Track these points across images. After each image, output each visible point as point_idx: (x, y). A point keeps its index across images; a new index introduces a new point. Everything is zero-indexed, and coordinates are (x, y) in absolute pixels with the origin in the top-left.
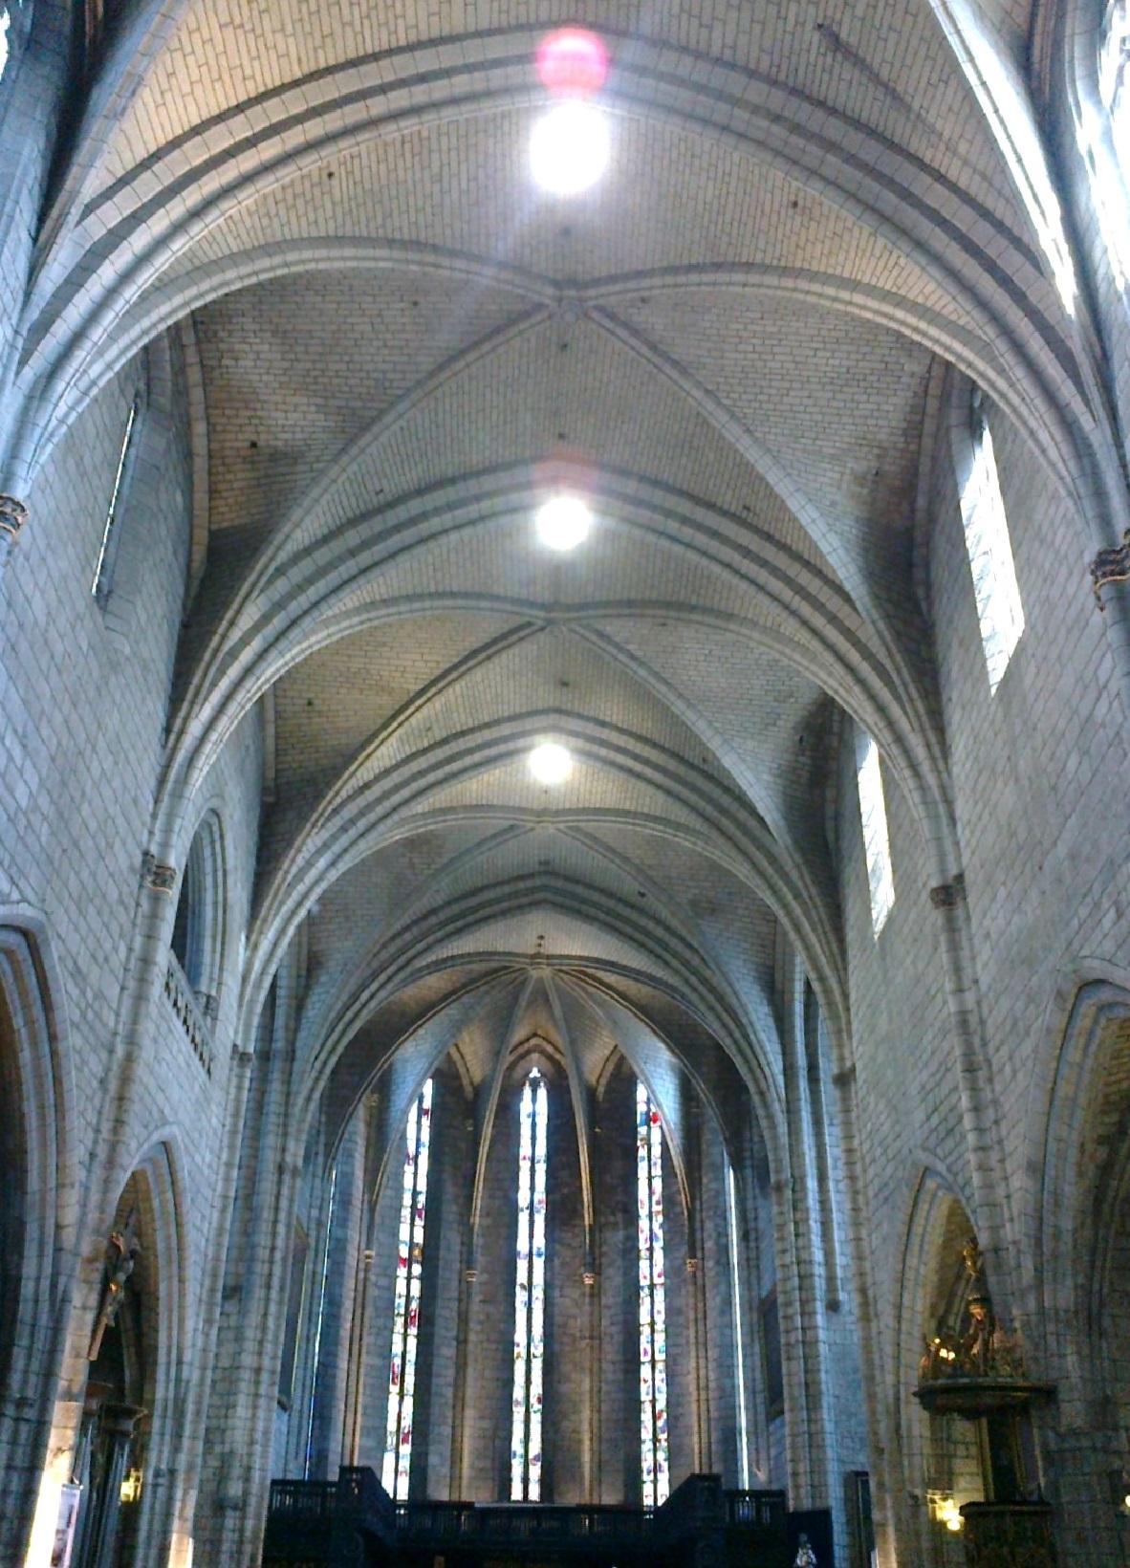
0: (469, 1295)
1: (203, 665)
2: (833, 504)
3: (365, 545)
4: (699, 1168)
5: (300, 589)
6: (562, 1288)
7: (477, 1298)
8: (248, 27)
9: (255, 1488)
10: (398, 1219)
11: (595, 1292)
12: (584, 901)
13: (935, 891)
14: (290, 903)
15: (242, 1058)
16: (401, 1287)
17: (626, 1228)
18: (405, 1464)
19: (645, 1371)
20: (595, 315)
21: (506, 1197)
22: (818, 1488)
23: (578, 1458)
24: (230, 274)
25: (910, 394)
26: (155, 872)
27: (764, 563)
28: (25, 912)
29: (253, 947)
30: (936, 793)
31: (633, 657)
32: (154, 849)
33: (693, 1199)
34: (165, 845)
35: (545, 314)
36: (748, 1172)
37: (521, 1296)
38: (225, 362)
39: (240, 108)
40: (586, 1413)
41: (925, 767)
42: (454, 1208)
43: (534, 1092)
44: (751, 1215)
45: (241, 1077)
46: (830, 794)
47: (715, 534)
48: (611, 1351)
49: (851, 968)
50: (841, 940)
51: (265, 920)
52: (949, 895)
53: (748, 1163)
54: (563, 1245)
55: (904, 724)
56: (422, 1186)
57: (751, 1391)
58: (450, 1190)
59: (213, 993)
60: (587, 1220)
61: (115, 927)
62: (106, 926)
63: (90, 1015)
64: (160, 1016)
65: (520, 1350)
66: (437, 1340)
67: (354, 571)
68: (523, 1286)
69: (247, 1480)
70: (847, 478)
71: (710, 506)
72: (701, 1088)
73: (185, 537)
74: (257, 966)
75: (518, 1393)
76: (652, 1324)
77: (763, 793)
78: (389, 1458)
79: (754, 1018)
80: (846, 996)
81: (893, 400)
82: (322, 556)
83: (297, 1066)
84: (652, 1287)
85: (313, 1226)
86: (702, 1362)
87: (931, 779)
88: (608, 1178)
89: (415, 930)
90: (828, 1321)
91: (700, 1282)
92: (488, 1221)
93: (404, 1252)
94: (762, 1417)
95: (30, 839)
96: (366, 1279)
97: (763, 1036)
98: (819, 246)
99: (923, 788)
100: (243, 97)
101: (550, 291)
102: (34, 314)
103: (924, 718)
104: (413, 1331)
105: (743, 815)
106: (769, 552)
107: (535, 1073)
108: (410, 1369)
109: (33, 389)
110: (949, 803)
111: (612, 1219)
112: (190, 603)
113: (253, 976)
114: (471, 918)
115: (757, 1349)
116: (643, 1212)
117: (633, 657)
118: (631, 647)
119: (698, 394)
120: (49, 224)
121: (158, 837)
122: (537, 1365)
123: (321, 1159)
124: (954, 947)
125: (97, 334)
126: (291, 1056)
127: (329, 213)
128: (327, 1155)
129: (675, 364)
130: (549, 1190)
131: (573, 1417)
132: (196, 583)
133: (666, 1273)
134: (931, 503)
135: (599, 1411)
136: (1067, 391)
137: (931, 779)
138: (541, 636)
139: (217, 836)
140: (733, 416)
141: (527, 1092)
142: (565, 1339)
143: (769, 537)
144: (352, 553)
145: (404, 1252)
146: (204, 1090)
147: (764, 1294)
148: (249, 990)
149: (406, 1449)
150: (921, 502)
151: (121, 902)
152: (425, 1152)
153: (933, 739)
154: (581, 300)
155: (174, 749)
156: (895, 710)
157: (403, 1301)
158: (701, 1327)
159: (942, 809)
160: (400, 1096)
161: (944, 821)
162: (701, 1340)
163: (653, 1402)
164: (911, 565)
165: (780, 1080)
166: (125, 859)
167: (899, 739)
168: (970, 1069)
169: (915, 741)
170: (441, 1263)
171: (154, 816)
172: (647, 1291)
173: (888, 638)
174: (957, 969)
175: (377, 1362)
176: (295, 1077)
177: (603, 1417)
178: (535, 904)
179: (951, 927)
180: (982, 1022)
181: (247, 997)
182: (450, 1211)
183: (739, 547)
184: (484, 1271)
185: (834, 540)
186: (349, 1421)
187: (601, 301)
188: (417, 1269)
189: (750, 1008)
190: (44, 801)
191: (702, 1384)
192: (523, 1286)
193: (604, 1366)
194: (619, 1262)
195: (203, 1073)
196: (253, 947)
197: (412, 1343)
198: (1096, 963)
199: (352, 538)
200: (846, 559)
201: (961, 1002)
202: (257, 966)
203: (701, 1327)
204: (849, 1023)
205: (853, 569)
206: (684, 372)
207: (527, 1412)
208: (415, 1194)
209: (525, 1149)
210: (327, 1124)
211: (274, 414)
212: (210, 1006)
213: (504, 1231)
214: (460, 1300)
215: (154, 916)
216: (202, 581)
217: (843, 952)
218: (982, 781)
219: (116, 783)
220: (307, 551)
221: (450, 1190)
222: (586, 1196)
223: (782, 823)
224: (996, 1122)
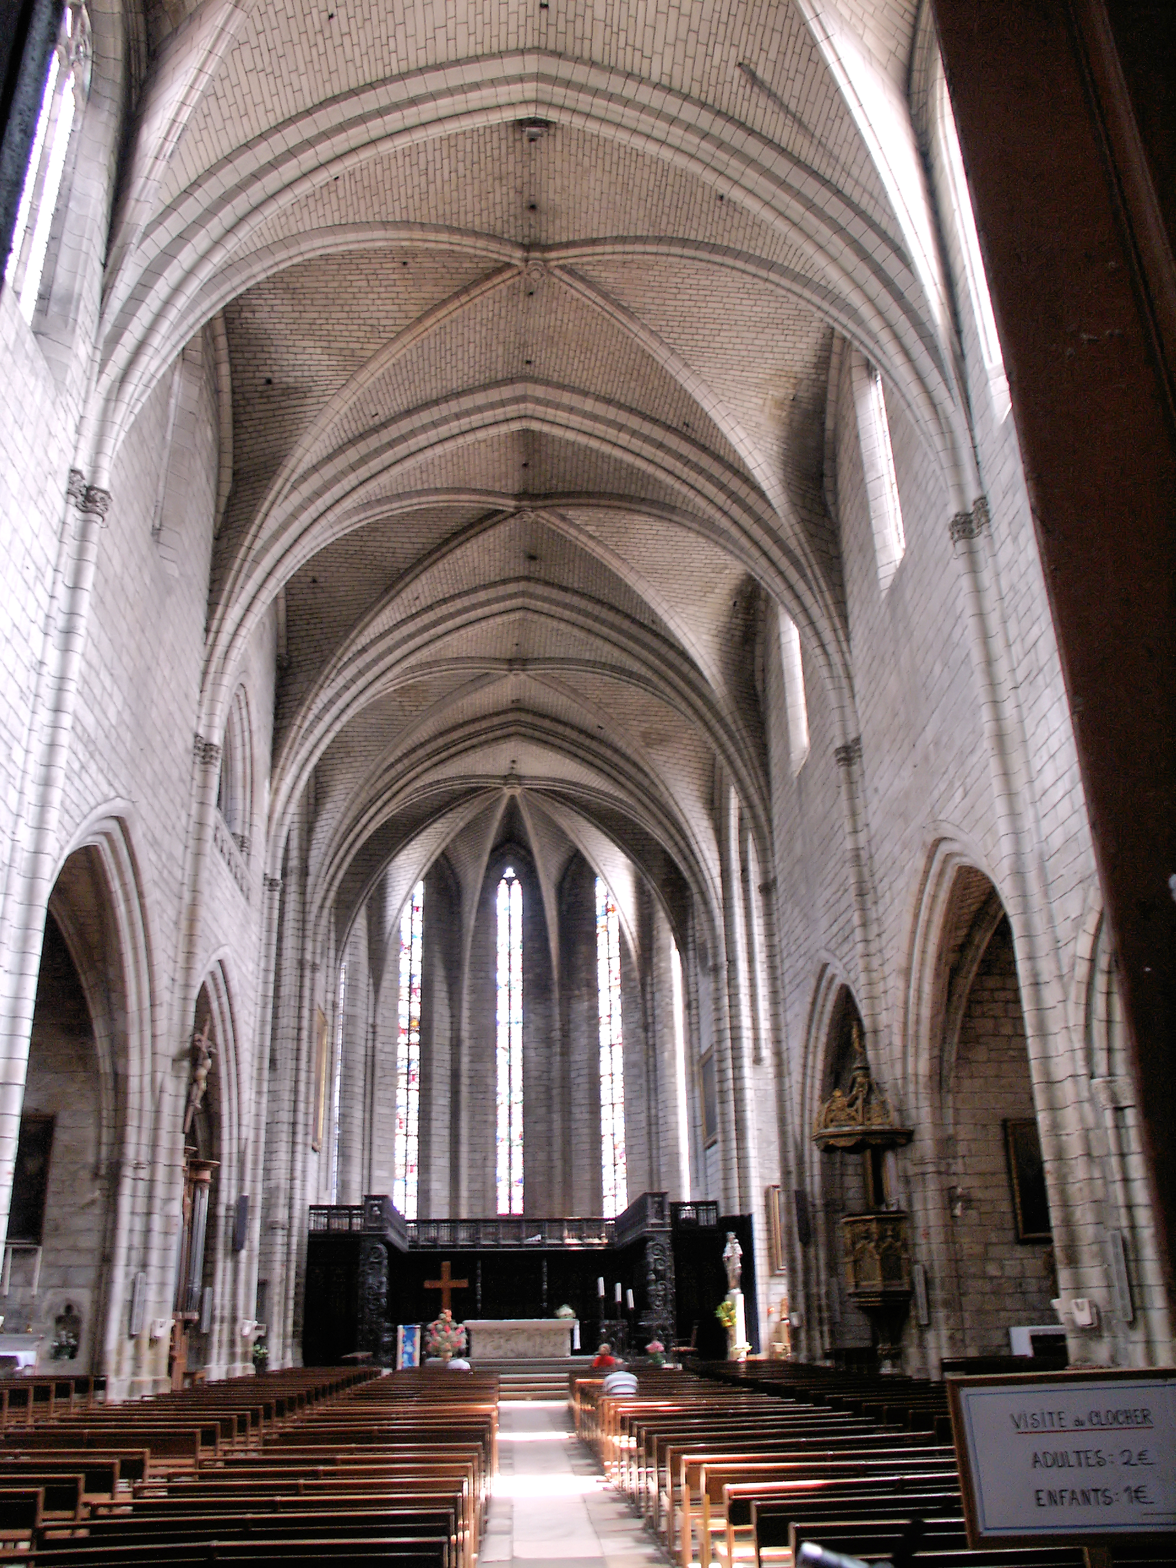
1: (233, 573)
2: (758, 425)
3: (363, 460)
5: (310, 500)
8: (269, 70)
9: (297, 1213)
10: (397, 997)
12: (548, 732)
13: (838, 751)
14: (303, 753)
15: (271, 883)
16: (402, 1052)
18: (413, 1189)
20: (558, 272)
22: (744, 1199)
24: (256, 268)
25: (820, 335)
26: (204, 750)
27: (701, 471)
28: (118, 806)
29: (276, 792)
30: (839, 670)
31: (591, 537)
32: (201, 732)
34: (210, 726)
35: (515, 271)
36: (691, 953)
38: (244, 315)
39: (263, 136)
41: (832, 648)
44: (692, 989)
45: (271, 899)
46: (759, 650)
47: (660, 446)
49: (775, 795)
50: (767, 774)
51: (283, 769)
52: (849, 754)
53: (691, 946)
55: (816, 611)
56: (417, 970)
57: (693, 1126)
59: (246, 834)
61: (178, 800)
62: (172, 801)
63: (165, 873)
64: (216, 868)
67: (355, 482)
69: (291, 1207)
70: (769, 403)
71: (655, 421)
72: (652, 886)
73: (214, 463)
74: (279, 808)
77: (703, 651)
78: (398, 1187)
79: (696, 830)
80: (770, 821)
81: (805, 339)
82: (328, 471)
83: (311, 880)
85: (329, 1007)
87: (836, 658)
89: (406, 762)
90: (755, 1071)
93: (404, 1024)
94: (700, 1148)
95: (120, 748)
96: (374, 1047)
97: (704, 846)
98: (741, 231)
99: (830, 665)
100: (265, 127)
101: (519, 254)
102: (107, 328)
103: (832, 608)
105: (686, 668)
106: (705, 461)
107: (510, 872)
108: (414, 1115)
109: (110, 392)
110: (849, 677)
112: (220, 517)
113: (276, 816)
114: (453, 750)
115: (697, 1093)
117: (591, 537)
118: (588, 528)
119: (644, 335)
120: (115, 251)
121: (204, 720)
123: (332, 953)
124: (852, 798)
125: (156, 341)
126: (304, 872)
127: (335, 207)
128: (337, 950)
129: (624, 309)
132: (223, 500)
134: (836, 424)
136: (934, 378)
137: (836, 658)
138: (512, 521)
139: (243, 704)
140: (673, 351)
143: (704, 449)
144: (353, 468)
145: (404, 1024)
146: (245, 915)
147: (703, 1051)
148: (274, 827)
149: (413, 1177)
150: (829, 424)
151: (182, 780)
152: (418, 943)
153: (838, 626)
154: (546, 261)
155: (214, 646)
156: (808, 599)
159: (844, 682)
160: (395, 899)
161: (846, 692)
164: (822, 475)
165: (718, 881)
166: (183, 743)
167: (812, 623)
168: (861, 894)
169: (823, 624)
170: (436, 1032)
171: (200, 703)
173: (803, 540)
174: (854, 814)
176: (309, 889)
178: (508, 736)
179: (851, 782)
180: (871, 857)
181: (272, 833)
183: (679, 457)
185: (760, 459)
187: (561, 262)
188: (415, 1037)
189: (693, 822)
190: (127, 716)
194: (584, 1028)
195: (241, 899)
196: (276, 792)
198: (949, 826)
199: (352, 455)
200: (769, 473)
201: (856, 841)
202: (279, 808)
204: (772, 844)
205: (774, 481)
206: (631, 315)
208: (411, 976)
210: (336, 923)
211: (285, 356)
212: (243, 843)
215: (204, 787)
216: (229, 499)
217: (768, 784)
218: (875, 665)
219: (173, 685)
220: (315, 468)
221: (440, 973)
222: (555, 975)
223: (719, 677)
224: (879, 935)
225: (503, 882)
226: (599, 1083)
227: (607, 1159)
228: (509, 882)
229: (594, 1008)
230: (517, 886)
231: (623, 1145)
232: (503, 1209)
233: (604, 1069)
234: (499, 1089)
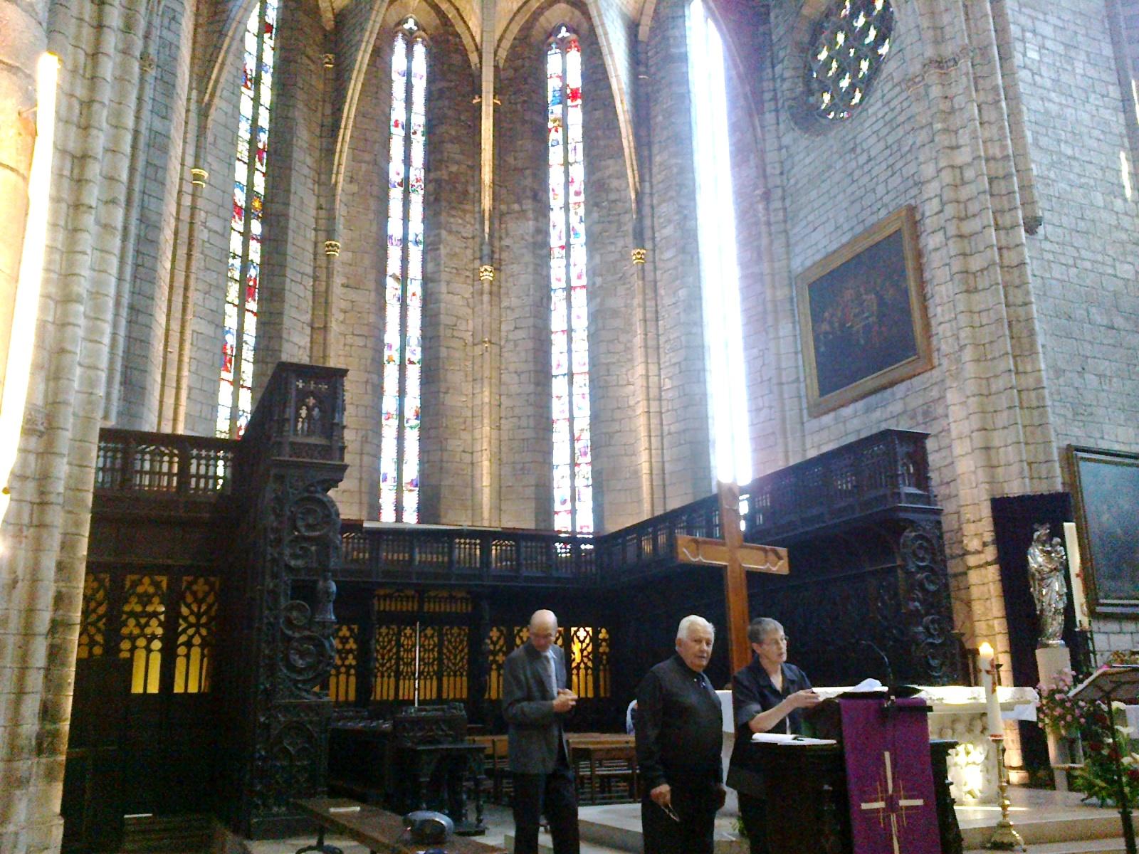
0: (329, 275)
4: (649, 145)
6: (448, 283)
7: (338, 280)
11: (496, 292)
17: (536, 219)
19: (559, 386)
21: (375, 163)
23: (471, 485)
33: (642, 180)
40: (485, 430)
42: (309, 161)
48: (517, 359)
54: (450, 232)
58: (303, 137)
60: (487, 203)
65: (391, 353)
66: (287, 322)
68: (394, 276)
75: (389, 403)
76: (569, 332)
84: (569, 289)
86: (653, 369)
88: (511, 160)
91: (649, 277)
92: (354, 188)
104: (252, 305)
108: (248, 354)
111: (516, 207)
116: (556, 202)
122: (414, 373)
130: (428, 167)
131: (466, 436)
133: (592, 272)
135: (499, 428)
141: (400, 45)
142: (456, 344)
157: (237, 263)
158: (652, 330)
162: (651, 343)
163: (571, 420)
170: (292, 224)
172: (563, 294)
175: (208, 330)
177: (505, 437)
182: (303, 161)
184: (347, 248)
186: (169, 401)
191: (654, 392)
192: (394, 276)
193: (505, 377)
194: (528, 258)
197: (251, 322)
203: (652, 330)
207: (401, 429)
209: (398, 113)
213: (373, 204)
214: (315, 278)
221: (303, 137)
222: (487, 175)
226: (550, 343)
227: (560, 454)
229: (543, 231)
230: (420, 50)
231: (586, 436)
232: (387, 517)
233: (557, 321)
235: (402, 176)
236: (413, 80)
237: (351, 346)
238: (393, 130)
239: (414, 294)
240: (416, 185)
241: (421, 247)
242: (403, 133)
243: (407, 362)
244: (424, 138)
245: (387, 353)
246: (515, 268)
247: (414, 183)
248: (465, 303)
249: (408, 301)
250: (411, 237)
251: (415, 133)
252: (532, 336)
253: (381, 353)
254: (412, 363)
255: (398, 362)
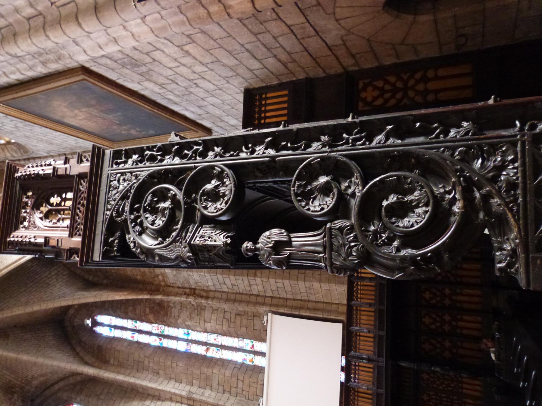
37: (213, 353)
43: (102, 325)
107: (89, 322)
141: (99, 330)
192: (207, 350)
209: (127, 335)
225: (94, 329)
228: (95, 323)
230: (100, 318)
234: (240, 360)
235: (156, 338)
236: (113, 324)
237: (243, 390)
238: (136, 340)
239: (215, 340)
240: (160, 330)
241: (190, 331)
242: (137, 334)
243: (252, 350)
244: (138, 322)
245: (248, 362)
246: (192, 281)
247: (159, 331)
248: (216, 312)
249: (219, 344)
250: (186, 337)
251: (136, 327)
252: (228, 276)
253: (248, 366)
254: (253, 346)
255: (252, 356)
